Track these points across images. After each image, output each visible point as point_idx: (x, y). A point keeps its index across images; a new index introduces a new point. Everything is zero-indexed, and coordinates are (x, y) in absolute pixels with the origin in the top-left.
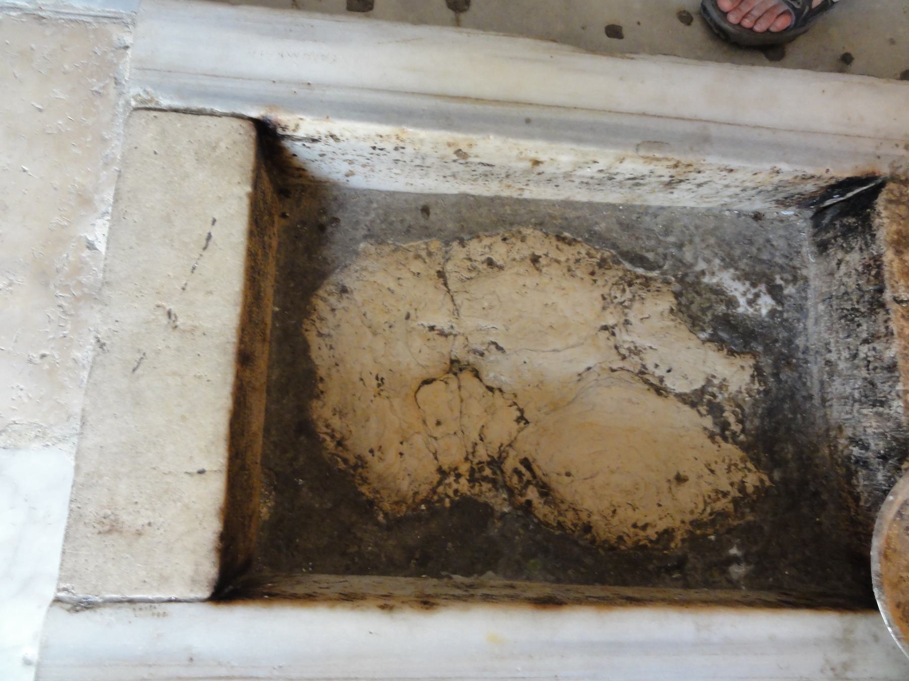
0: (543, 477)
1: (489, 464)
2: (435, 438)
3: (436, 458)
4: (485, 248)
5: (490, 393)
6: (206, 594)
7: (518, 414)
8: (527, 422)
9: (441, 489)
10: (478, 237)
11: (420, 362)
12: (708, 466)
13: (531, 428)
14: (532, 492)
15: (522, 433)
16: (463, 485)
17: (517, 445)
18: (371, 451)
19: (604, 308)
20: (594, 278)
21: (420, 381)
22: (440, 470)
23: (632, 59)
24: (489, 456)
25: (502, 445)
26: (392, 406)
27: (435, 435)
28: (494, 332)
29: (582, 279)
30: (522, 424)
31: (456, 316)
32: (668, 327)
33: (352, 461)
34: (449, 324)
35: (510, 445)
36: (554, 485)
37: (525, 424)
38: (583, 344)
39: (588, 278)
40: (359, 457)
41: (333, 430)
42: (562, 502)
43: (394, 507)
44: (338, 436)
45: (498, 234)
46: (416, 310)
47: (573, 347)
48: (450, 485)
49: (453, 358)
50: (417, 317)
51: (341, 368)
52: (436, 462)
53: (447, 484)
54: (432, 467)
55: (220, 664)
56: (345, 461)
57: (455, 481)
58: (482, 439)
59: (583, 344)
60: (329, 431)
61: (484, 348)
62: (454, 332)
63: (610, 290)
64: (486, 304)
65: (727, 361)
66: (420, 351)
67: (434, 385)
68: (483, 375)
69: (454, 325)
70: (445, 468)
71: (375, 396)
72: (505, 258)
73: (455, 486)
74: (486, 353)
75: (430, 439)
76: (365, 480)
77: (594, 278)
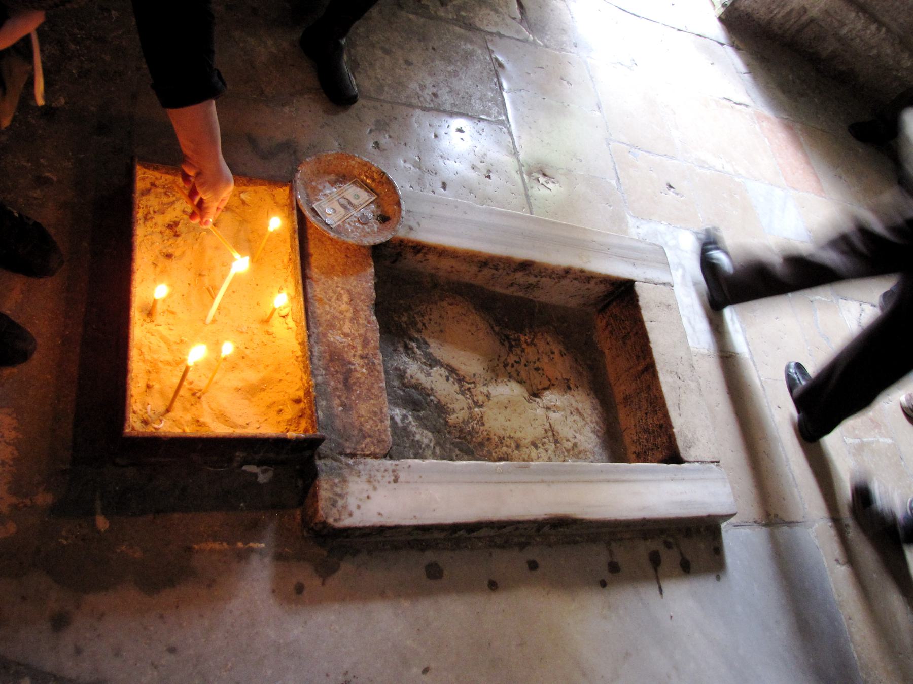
6: (636, 283)
12: (426, 328)
16: (523, 338)
18: (565, 354)
19: (482, 417)
20: (488, 436)
23: (546, 515)
29: (495, 435)
32: (451, 404)
39: (492, 436)
48: (529, 338)
55: (626, 262)
63: (480, 429)
65: (420, 381)
71: (570, 379)
73: (527, 338)
77: (488, 436)
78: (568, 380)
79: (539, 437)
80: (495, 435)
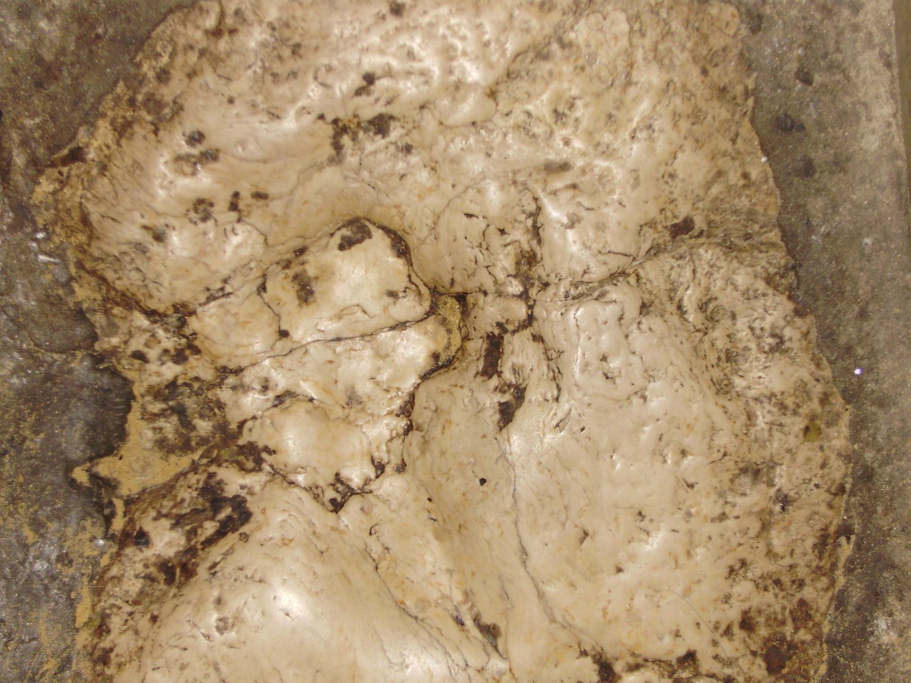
0: (208, 564)
1: (222, 427)
2: (263, 288)
3: (211, 298)
4: (773, 335)
5: (398, 403)
7: (356, 481)
8: (337, 506)
9: (141, 320)
10: (798, 313)
11: (443, 221)
13: (323, 518)
14: (170, 544)
15: (306, 497)
17: (278, 492)
20: (736, 629)
21: (395, 224)
22: (184, 312)
24: (242, 425)
25: (272, 452)
26: (320, 168)
27: (269, 285)
28: (549, 396)
29: (727, 599)
30: (330, 494)
31: (573, 292)
33: (167, 93)
34: (553, 279)
35: (275, 472)
36: (192, 592)
37: (333, 501)
38: (553, 620)
39: (733, 613)
40: (178, 109)
41: (233, 32)
42: (154, 619)
43: (76, 214)
44: (223, 45)
45: (818, 365)
46: (574, 186)
47: (541, 595)
49: (470, 299)
50: (554, 193)
51: (393, 23)
52: (203, 299)
53: (153, 335)
54: (185, 291)
56: (163, 76)
57: (166, 351)
58: (280, 399)
59: (553, 620)
60: (229, 21)
61: (508, 376)
62: (533, 292)
64: (614, 364)
66: (469, 216)
67: (399, 264)
68: (440, 382)
69: (551, 290)
70: (194, 324)
71: (335, 122)
72: (752, 393)
74: (494, 381)
75: (256, 273)
76: (123, 130)
77: (736, 629)
78: (340, 129)
79: (687, 346)
80: (727, 599)
